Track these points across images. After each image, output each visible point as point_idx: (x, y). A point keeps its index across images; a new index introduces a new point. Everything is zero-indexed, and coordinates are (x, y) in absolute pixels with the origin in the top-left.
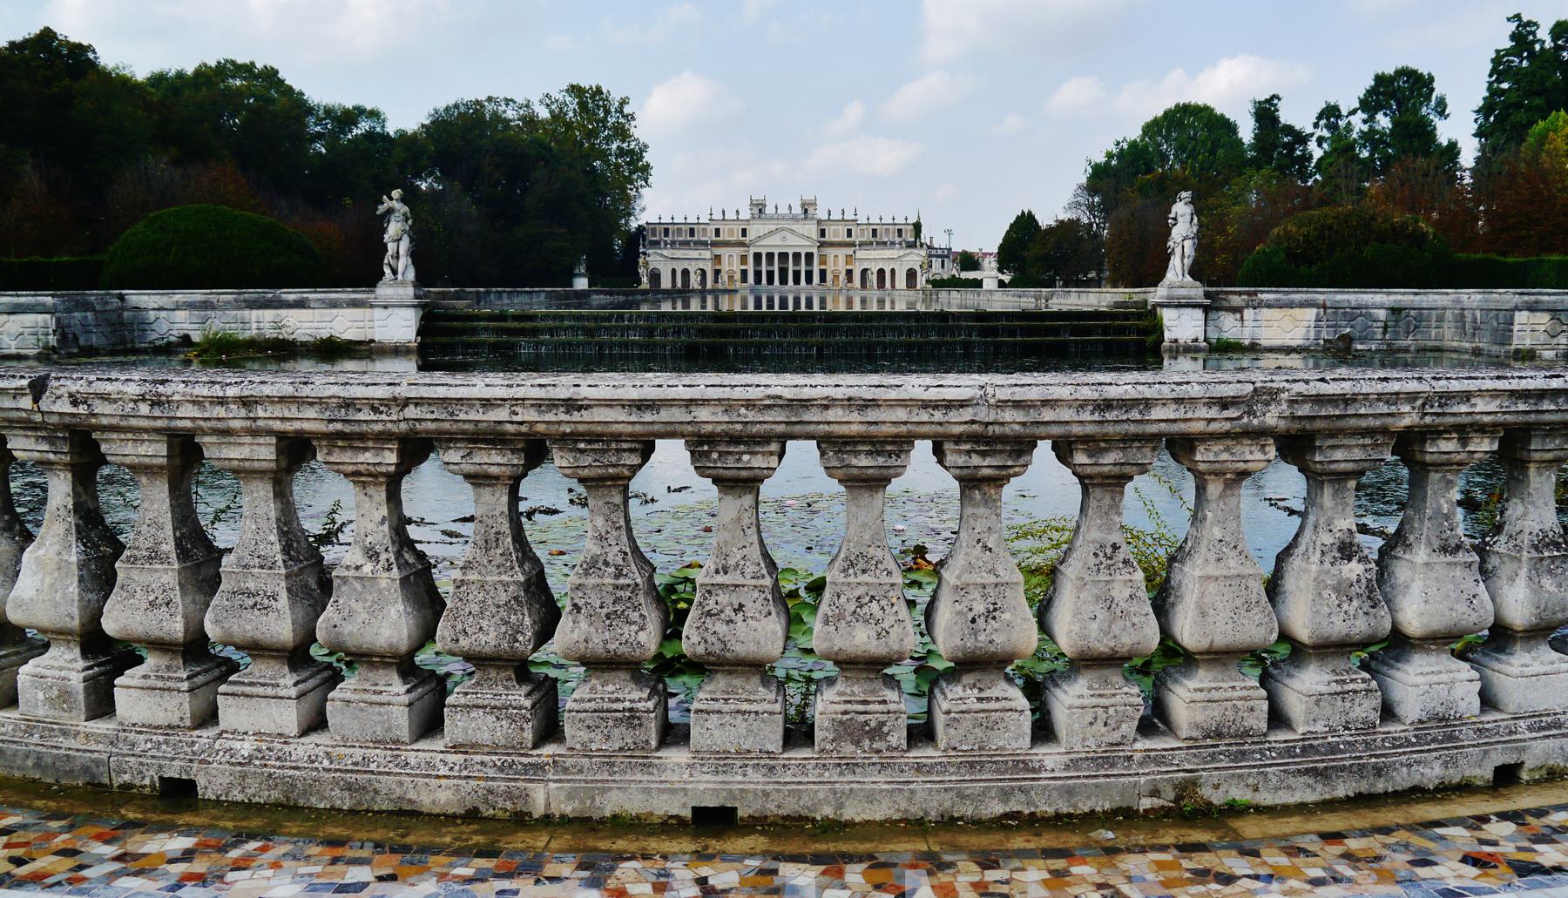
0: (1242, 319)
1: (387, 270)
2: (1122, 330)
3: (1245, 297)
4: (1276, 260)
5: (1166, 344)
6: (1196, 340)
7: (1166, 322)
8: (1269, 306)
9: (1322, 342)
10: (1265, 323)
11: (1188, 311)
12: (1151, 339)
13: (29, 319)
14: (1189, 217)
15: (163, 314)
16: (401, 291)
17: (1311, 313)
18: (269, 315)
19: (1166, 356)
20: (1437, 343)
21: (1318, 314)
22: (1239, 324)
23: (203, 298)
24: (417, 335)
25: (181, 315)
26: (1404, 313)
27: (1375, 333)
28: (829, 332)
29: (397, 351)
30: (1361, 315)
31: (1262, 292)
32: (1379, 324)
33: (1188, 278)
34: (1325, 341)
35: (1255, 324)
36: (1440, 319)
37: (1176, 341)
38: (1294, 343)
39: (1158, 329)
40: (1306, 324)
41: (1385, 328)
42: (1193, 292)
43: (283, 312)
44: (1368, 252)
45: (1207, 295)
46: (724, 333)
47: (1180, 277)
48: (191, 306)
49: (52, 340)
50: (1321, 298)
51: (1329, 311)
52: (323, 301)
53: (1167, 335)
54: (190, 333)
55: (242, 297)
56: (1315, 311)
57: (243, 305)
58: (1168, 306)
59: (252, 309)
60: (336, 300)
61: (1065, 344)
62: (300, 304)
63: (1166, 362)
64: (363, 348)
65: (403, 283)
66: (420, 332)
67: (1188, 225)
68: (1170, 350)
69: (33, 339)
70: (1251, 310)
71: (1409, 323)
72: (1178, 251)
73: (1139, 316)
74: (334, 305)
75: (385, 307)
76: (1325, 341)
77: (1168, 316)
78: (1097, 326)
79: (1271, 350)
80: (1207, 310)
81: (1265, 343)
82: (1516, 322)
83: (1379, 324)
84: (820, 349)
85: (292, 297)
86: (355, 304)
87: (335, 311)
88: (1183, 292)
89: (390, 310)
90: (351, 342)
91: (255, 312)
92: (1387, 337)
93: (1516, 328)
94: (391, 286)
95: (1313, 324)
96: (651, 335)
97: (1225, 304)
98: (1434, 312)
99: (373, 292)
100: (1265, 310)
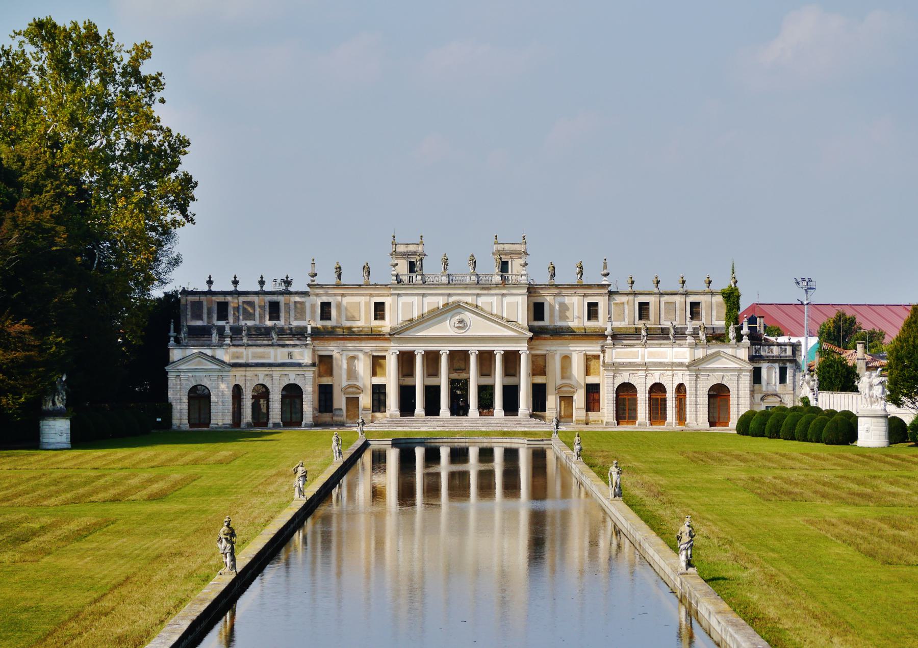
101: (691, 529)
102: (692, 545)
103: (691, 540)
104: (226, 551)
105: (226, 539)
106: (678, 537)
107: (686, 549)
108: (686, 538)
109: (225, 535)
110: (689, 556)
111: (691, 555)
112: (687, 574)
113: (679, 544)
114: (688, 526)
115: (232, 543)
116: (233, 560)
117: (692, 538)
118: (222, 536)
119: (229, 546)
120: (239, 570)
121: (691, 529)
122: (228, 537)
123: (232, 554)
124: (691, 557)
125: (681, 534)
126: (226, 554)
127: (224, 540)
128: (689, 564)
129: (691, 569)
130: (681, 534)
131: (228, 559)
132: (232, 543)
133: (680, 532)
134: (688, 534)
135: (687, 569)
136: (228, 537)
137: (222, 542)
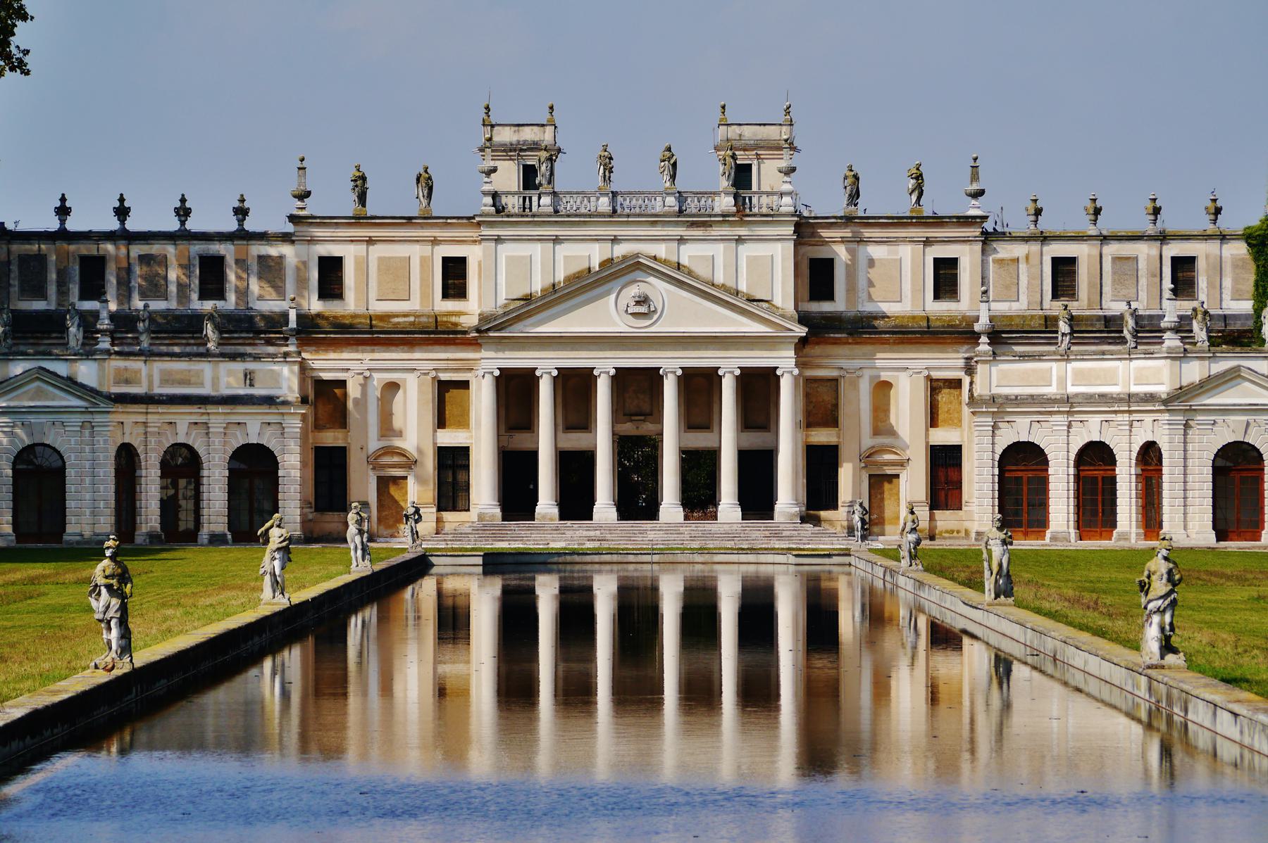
101: (1171, 565)
102: (1174, 603)
103: (1171, 592)
104: (108, 616)
105: (109, 587)
107: (1159, 611)
108: (1159, 587)
109: (106, 577)
110: (1168, 627)
111: (1171, 624)
112: (1163, 667)
113: (1143, 600)
114: (1166, 559)
115: (123, 597)
116: (126, 634)
117: (1174, 585)
118: (101, 580)
119: (115, 603)
120: (138, 664)
121: (1171, 565)
122: (114, 582)
123: (123, 622)
124: (1172, 628)
125: (1149, 577)
126: (109, 622)
127: (104, 590)
128: (1167, 647)
129: (1170, 658)
130: (1149, 577)
131: (115, 633)
132: (123, 597)
133: (1146, 573)
134: (1165, 576)
135: (1162, 658)
136: (114, 582)
137: (99, 594)
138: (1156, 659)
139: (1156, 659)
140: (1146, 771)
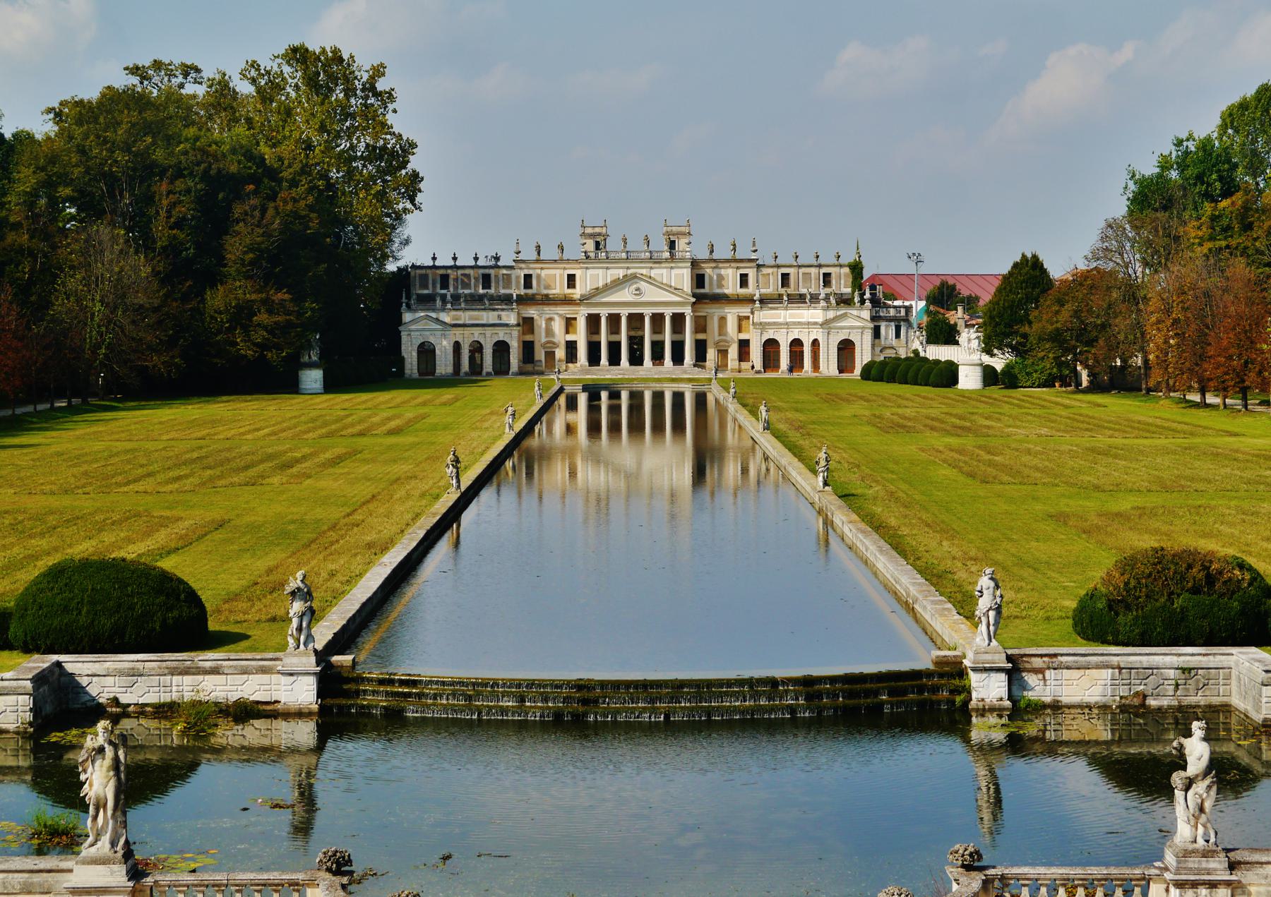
0: (1044, 678)
1: (291, 641)
2: (935, 689)
3: (1046, 659)
4: (1100, 606)
5: (973, 704)
6: (1001, 699)
7: (974, 684)
8: (1068, 668)
9: (1118, 698)
10: (1064, 682)
11: (994, 675)
12: (959, 699)
13: (11, 699)
14: (991, 590)
15: (95, 679)
16: (304, 659)
17: (1107, 674)
18: (188, 679)
19: (974, 714)
20: (1225, 699)
21: (1113, 674)
22: (1042, 683)
23: (131, 665)
24: (317, 698)
25: (109, 681)
26: (1193, 672)
27: (1166, 690)
28: (674, 698)
29: (300, 714)
30: (1152, 674)
31: (1062, 655)
32: (1170, 682)
33: (994, 643)
34: (1121, 698)
35: (1056, 683)
36: (1228, 677)
37: (983, 700)
38: (1093, 700)
39: (968, 691)
40: (1103, 682)
41: (1177, 685)
42: (997, 657)
43: (200, 678)
44: (1178, 603)
45: (1009, 658)
46: (585, 702)
47: (987, 642)
48: (121, 673)
49: (29, 717)
50: (1116, 659)
51: (1124, 671)
52: (235, 667)
53: (974, 695)
54: (118, 695)
55: (164, 664)
56: (1110, 671)
57: (166, 671)
58: (975, 670)
59: (173, 675)
60: (247, 667)
61: (882, 703)
62: (215, 671)
63: (974, 720)
64: (269, 708)
65: (305, 654)
66: (320, 694)
67: (991, 597)
68: (977, 710)
69: (13, 717)
70: (1052, 671)
71: (1198, 681)
72: (984, 620)
73: (951, 676)
74: (245, 672)
75: (291, 675)
76: (1121, 698)
77: (974, 679)
78: (913, 687)
79: (1070, 707)
80: (1009, 672)
81: (1065, 700)
82: (1264, 695)
83: (1170, 682)
84: (667, 717)
85: (208, 664)
86: (264, 671)
87: (245, 676)
88: (988, 657)
89: (294, 678)
90: (258, 702)
91: (175, 678)
92: (1179, 693)
93: (1264, 700)
94: (296, 655)
95: (1109, 682)
96: (522, 700)
97: (1027, 666)
98: (1221, 671)
99: (281, 660)
100: (1065, 671)
105: (453, 465)
106: (817, 462)
107: (823, 472)
108: (823, 463)
115: (457, 468)
116: (458, 481)
119: (455, 470)
120: (463, 490)
128: (826, 484)
129: (827, 488)
131: (454, 481)
132: (457, 468)
138: (821, 488)
139: (821, 488)
140: (819, 534)
